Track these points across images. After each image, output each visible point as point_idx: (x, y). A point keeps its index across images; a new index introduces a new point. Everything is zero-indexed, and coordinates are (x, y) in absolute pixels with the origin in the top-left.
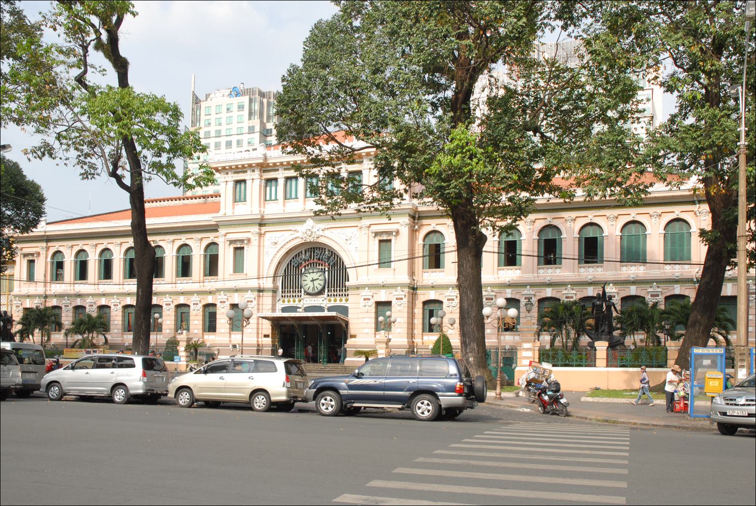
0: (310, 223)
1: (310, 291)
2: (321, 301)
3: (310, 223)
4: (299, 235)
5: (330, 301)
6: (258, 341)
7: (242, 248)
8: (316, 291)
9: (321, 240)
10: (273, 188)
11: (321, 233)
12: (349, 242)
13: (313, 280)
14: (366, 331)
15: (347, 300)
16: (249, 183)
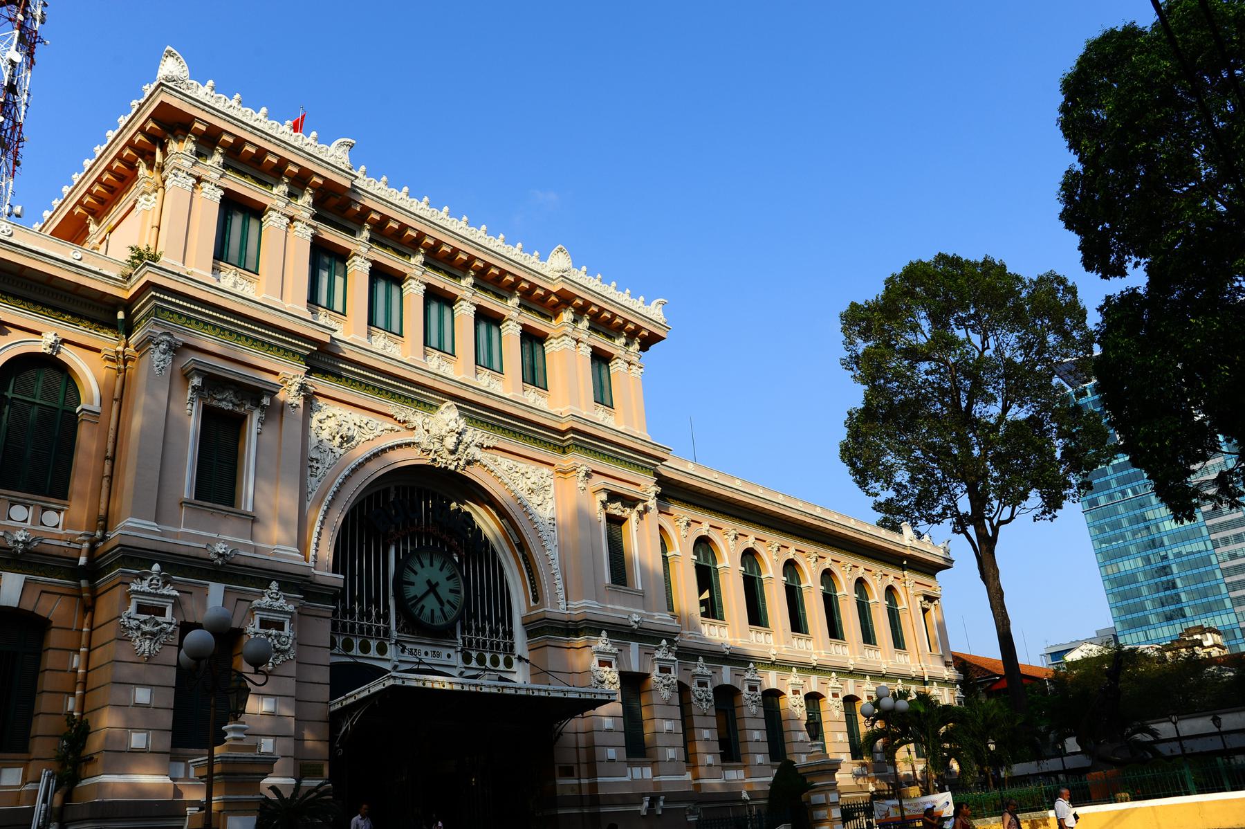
0: (448, 417)
1: (425, 617)
2: (444, 660)
3: (448, 417)
4: (419, 436)
5: (467, 659)
6: (297, 787)
7: (238, 422)
8: (440, 622)
9: (473, 473)
10: (324, 276)
11: (478, 454)
12: (535, 500)
13: (432, 588)
14: (611, 753)
15: (509, 663)
16: (273, 222)
